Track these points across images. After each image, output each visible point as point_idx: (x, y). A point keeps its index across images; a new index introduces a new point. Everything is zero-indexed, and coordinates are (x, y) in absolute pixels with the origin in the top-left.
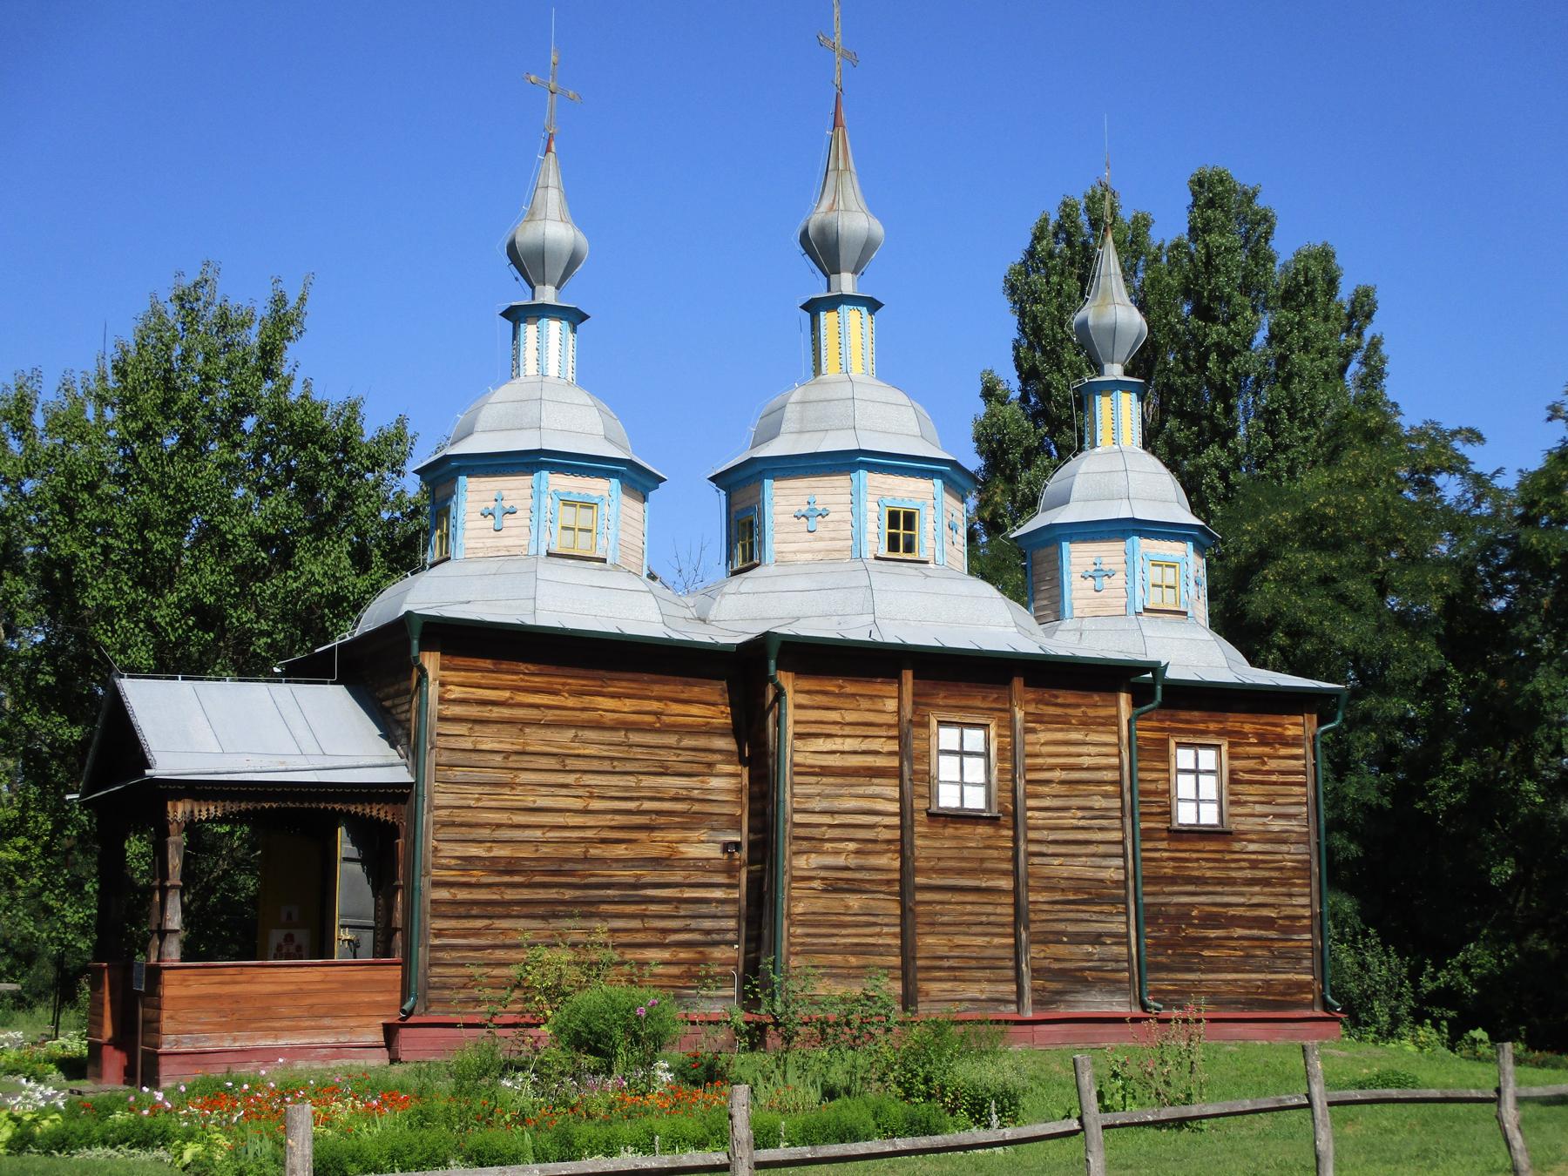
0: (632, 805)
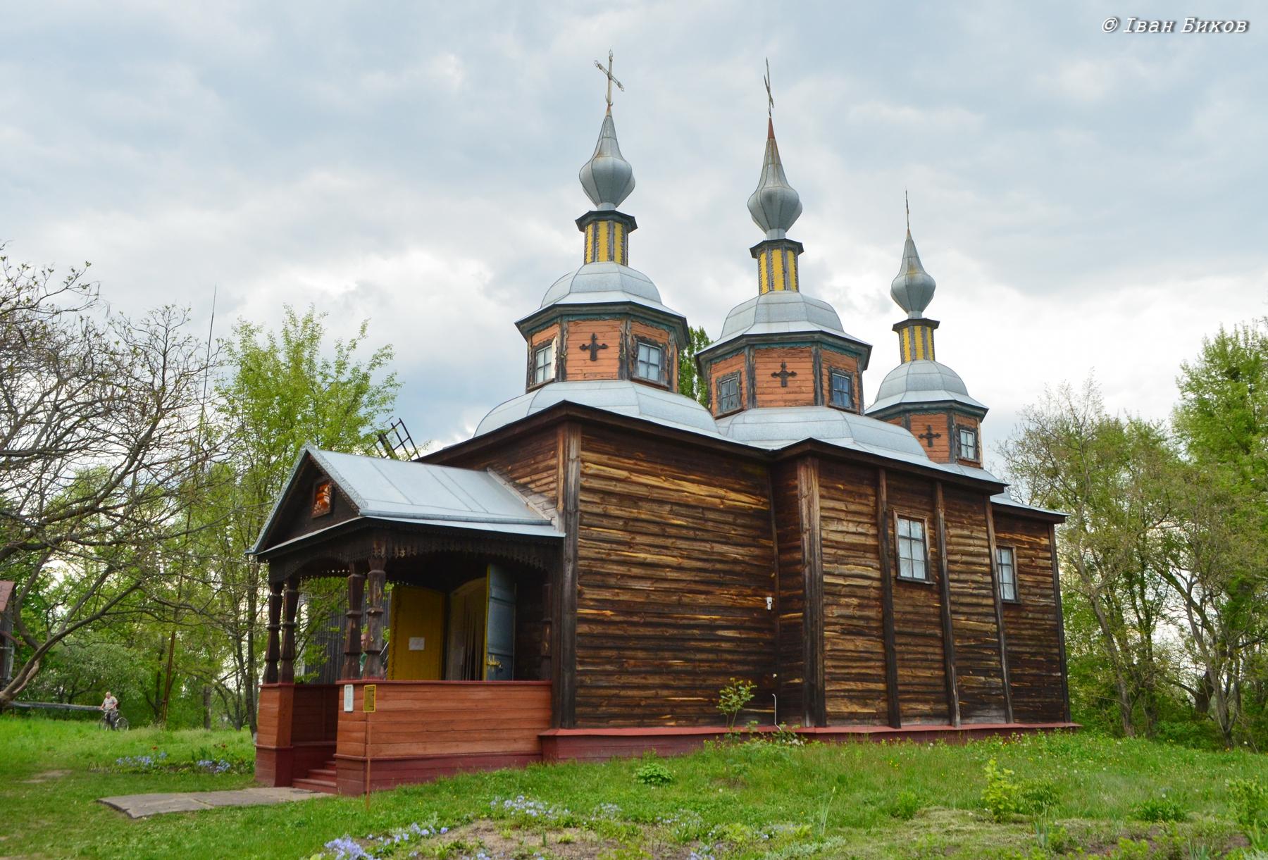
0: (707, 565)
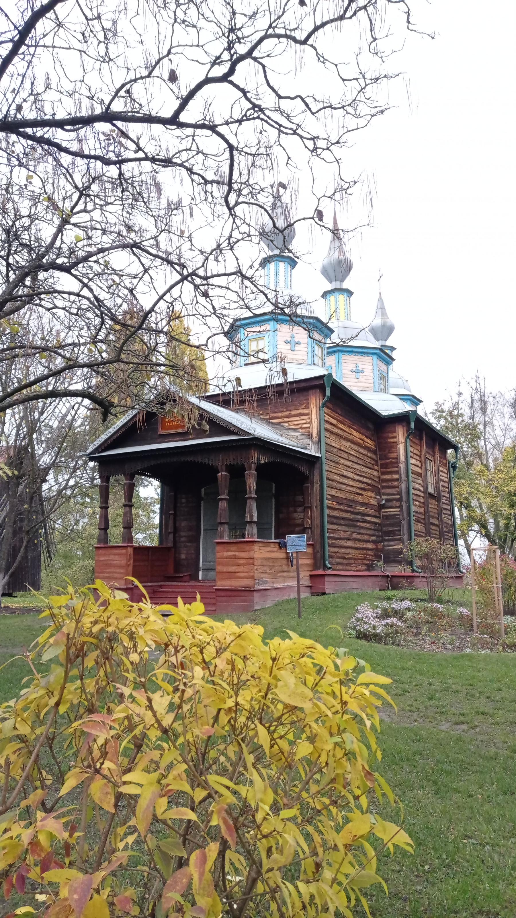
0: (361, 479)
